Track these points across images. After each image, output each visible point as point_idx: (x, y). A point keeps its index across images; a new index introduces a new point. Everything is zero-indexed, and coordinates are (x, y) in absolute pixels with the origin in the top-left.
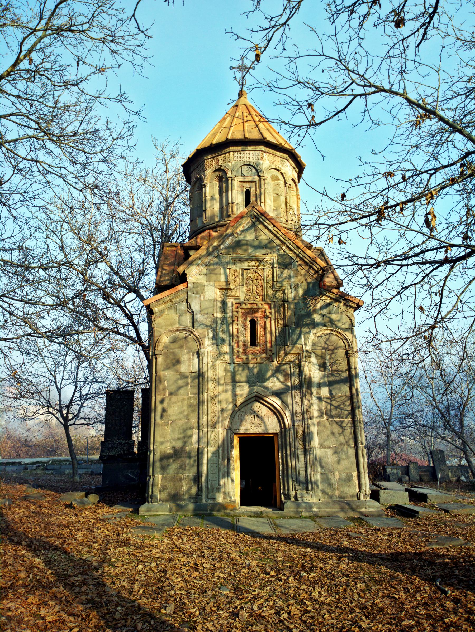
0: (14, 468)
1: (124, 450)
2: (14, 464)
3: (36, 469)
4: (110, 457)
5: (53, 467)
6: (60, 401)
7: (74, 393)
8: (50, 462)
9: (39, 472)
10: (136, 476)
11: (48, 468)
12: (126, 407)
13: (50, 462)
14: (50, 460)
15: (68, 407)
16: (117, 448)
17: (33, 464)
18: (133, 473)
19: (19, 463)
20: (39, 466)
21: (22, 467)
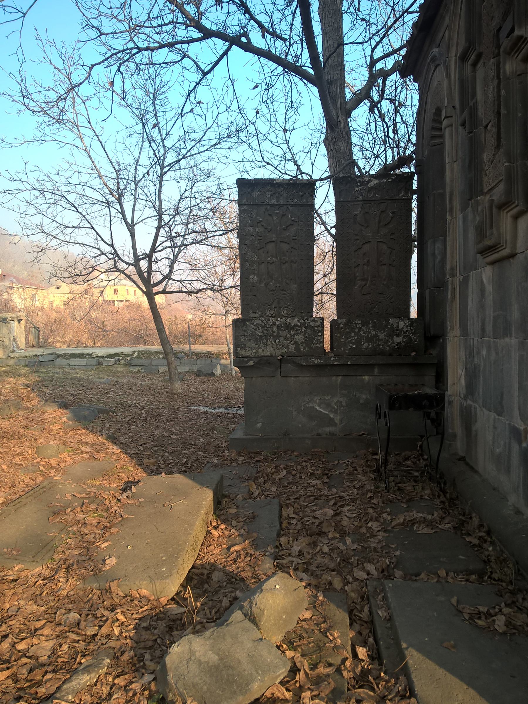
0: (82, 362)
1: (296, 343)
2: (81, 356)
4: (263, 362)
5: (139, 361)
6: (134, 247)
7: (158, 229)
8: (136, 355)
9: (120, 369)
10: (335, 412)
11: (133, 362)
12: (293, 229)
13: (136, 355)
14: (134, 352)
15: (149, 256)
16: (278, 337)
17: (110, 356)
18: (328, 405)
19: (90, 355)
20: (119, 360)
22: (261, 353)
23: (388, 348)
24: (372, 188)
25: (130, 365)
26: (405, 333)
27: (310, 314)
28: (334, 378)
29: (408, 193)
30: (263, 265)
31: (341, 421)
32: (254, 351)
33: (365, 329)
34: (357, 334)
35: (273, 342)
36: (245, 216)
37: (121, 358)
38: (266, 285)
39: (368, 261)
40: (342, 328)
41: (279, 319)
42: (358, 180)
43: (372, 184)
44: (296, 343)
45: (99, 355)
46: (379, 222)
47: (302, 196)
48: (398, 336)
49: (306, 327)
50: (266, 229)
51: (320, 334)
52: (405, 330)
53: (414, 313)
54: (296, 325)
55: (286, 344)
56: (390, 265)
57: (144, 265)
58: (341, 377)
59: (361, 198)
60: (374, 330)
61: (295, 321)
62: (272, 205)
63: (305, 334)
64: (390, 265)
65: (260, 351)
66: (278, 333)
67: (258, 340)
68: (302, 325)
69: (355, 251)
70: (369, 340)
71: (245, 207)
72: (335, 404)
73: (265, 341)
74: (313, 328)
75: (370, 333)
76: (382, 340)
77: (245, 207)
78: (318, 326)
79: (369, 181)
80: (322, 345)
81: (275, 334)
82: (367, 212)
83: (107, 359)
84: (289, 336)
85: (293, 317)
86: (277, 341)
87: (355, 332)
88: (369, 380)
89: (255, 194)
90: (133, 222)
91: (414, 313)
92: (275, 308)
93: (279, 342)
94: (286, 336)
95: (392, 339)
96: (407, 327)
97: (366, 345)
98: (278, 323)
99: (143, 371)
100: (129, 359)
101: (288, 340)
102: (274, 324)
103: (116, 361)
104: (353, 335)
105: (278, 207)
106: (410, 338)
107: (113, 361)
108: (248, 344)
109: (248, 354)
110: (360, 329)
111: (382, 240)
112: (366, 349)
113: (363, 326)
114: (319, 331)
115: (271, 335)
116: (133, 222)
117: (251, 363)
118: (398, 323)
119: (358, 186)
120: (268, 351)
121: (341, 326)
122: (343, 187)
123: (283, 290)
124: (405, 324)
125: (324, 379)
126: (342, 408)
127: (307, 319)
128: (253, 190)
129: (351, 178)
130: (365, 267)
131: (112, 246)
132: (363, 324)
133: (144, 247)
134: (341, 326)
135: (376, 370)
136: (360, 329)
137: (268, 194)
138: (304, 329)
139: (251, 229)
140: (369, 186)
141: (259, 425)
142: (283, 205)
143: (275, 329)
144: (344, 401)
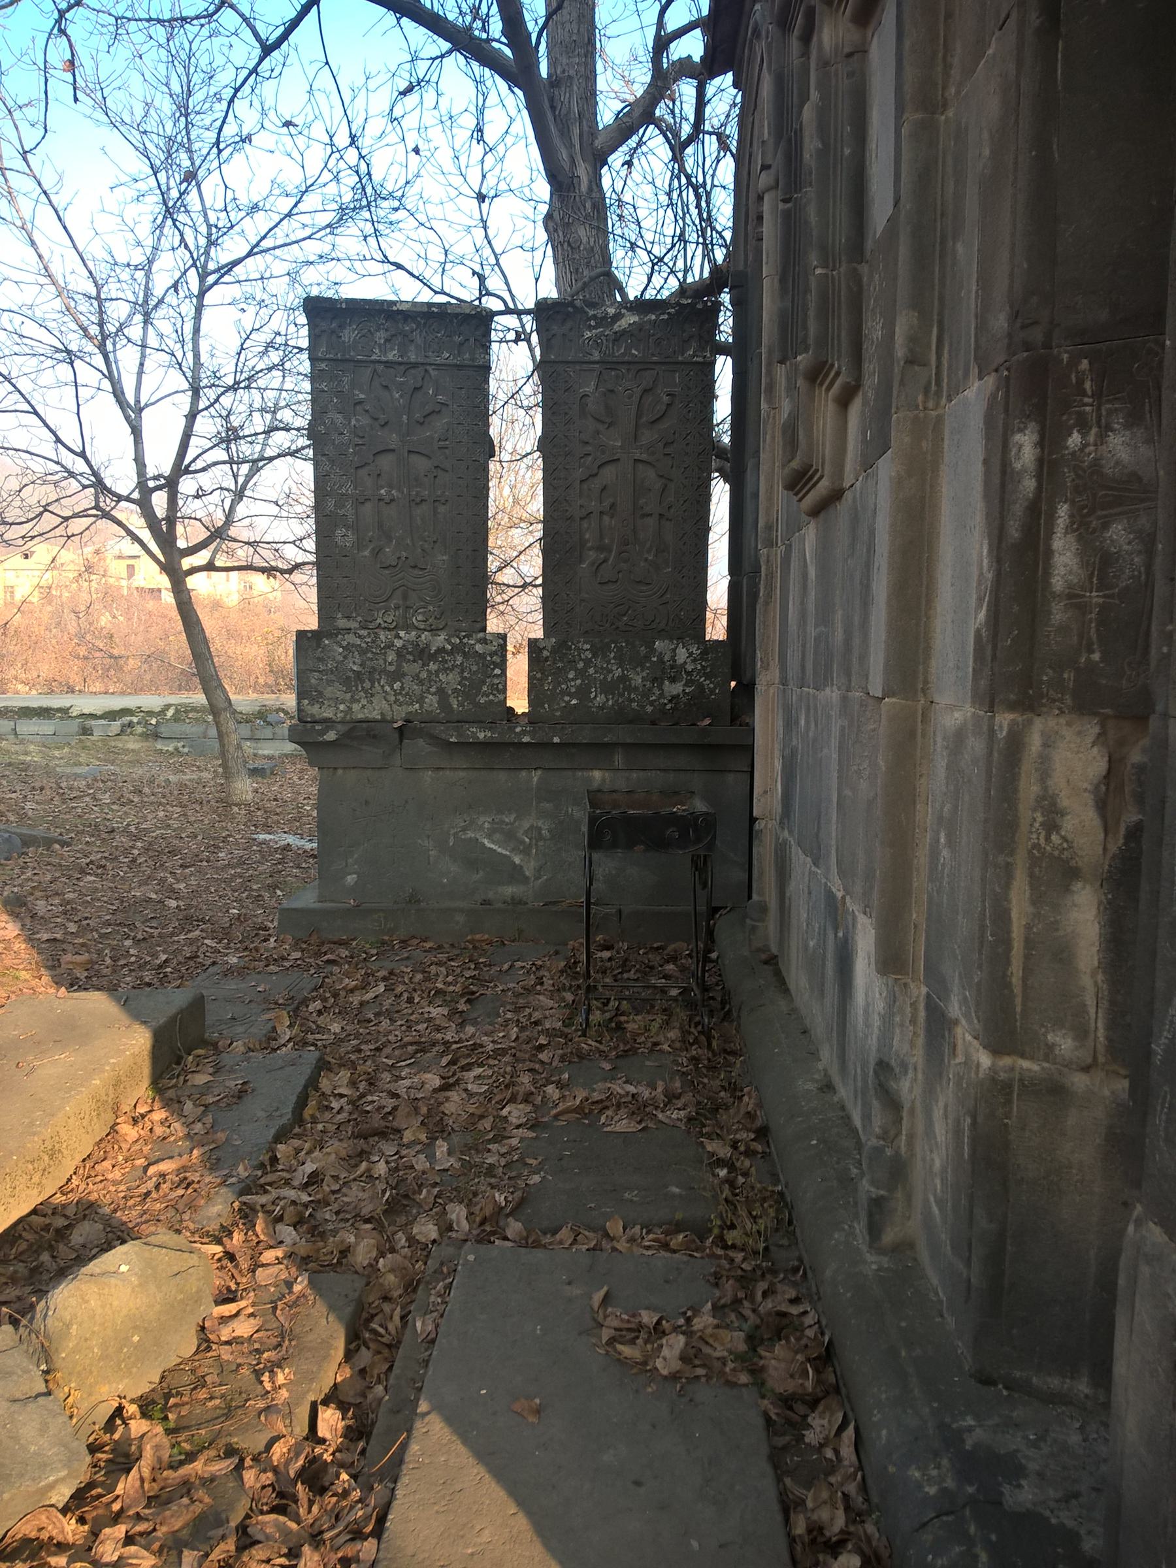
0: (46, 727)
1: (441, 692)
2: (44, 713)
3: (122, 732)
4: (360, 734)
5: (178, 729)
6: (140, 461)
7: (191, 417)
8: (170, 713)
9: (132, 744)
10: (526, 851)
11: (164, 731)
12: (440, 423)
13: (170, 713)
16: (398, 675)
17: (111, 715)
18: (509, 836)
19: (65, 711)
20: (130, 725)
21: (74, 726)
22: (359, 711)
23: (649, 709)
24: (623, 333)
25: (157, 736)
26: (689, 673)
27: (478, 626)
28: (524, 773)
29: (704, 349)
30: (368, 505)
31: (539, 871)
32: (342, 707)
33: (598, 662)
34: (581, 674)
35: (387, 688)
36: (324, 386)
37: (135, 720)
38: (377, 552)
39: (613, 506)
40: (546, 659)
41: (402, 634)
42: (591, 313)
44: (441, 692)
45: (86, 711)
46: (639, 416)
47: (461, 344)
48: (673, 680)
49: (465, 655)
50: (376, 419)
51: (497, 671)
52: (689, 668)
53: (717, 629)
54: (441, 650)
55: (418, 692)
57: (159, 501)
58: (539, 772)
59: (596, 356)
60: (620, 665)
61: (440, 640)
62: (389, 364)
63: (462, 671)
65: (356, 707)
66: (399, 666)
67: (352, 682)
68: (456, 649)
70: (608, 688)
71: (323, 366)
72: (526, 833)
73: (367, 685)
74: (482, 656)
75: (610, 671)
76: (636, 688)
77: (323, 366)
78: (492, 654)
79: (617, 317)
80: (501, 697)
81: (392, 668)
82: (612, 391)
83: (103, 722)
84: (424, 675)
85: (434, 631)
86: (397, 685)
87: (576, 670)
88: (604, 780)
89: (349, 335)
90: (138, 401)
91: (717, 629)
92: (397, 608)
93: (402, 688)
94: (417, 675)
97: (601, 699)
98: (398, 643)
99: (186, 750)
100: (154, 721)
101: (421, 682)
102: (390, 646)
103: (123, 726)
104: (571, 676)
105: (402, 368)
106: (701, 687)
107: (116, 726)
108: (329, 691)
109: (328, 714)
110: (588, 662)
111: (644, 457)
112: (602, 708)
114: (496, 665)
115: (384, 671)
116: (138, 401)
117: (331, 736)
118: (674, 650)
119: (590, 328)
120: (374, 707)
121: (546, 653)
122: (555, 328)
123: (415, 567)
124: (691, 654)
125: (502, 776)
126: (541, 843)
127: (468, 636)
128: (342, 327)
129: (574, 307)
130: (606, 518)
131: (82, 455)
132: (595, 652)
133: (160, 461)
134: (546, 653)
135: (619, 759)
136: (588, 662)
137: (380, 336)
138: (459, 659)
139: (339, 419)
140: (616, 327)
141: (351, 879)
142: (415, 365)
143: (391, 656)
144: (545, 826)
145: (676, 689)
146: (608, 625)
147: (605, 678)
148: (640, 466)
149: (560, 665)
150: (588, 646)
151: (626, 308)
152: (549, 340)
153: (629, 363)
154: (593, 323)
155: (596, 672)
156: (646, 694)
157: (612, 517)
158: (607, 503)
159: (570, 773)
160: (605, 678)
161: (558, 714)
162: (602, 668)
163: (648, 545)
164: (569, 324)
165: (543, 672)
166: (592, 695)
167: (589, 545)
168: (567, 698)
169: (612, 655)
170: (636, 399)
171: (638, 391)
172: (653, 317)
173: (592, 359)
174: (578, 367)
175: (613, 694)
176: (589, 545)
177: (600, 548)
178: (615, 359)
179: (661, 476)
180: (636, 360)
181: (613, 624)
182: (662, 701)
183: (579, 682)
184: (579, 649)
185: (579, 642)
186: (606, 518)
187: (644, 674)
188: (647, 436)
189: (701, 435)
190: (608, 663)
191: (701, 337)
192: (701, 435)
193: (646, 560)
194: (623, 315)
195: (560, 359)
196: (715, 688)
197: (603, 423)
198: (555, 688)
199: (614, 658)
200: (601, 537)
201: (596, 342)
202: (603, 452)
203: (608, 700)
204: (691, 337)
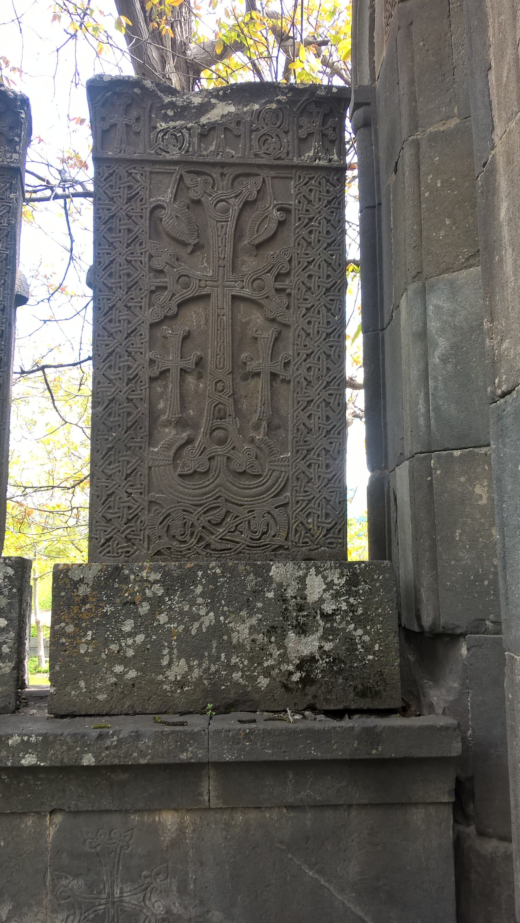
23: (263, 682)
24: (212, 127)
28: (29, 821)
29: (327, 151)
33: (176, 602)
34: (144, 624)
39: (199, 362)
40: (84, 600)
42: (167, 100)
43: (214, 115)
48: (302, 630)
52: (329, 608)
53: (358, 547)
56: (274, 376)
58: (58, 818)
59: (175, 154)
60: (212, 607)
64: (274, 376)
69: (153, 326)
70: (192, 648)
75: (196, 618)
76: (239, 647)
79: (204, 108)
82: (198, 202)
87: (136, 616)
88: (181, 829)
91: (358, 547)
95: (281, 646)
96: (336, 596)
97: (180, 667)
104: (128, 626)
106: (350, 641)
110: (157, 604)
111: (247, 292)
112: (180, 684)
113: (169, 591)
118: (302, 580)
119: (166, 118)
121: (83, 590)
124: (330, 585)
129: (143, 88)
132: (170, 583)
134: (83, 590)
135: (209, 789)
136: (157, 604)
140: (204, 120)
145: (309, 645)
146: (194, 540)
147: (187, 630)
148: (242, 307)
149: (108, 609)
150: (153, 577)
151: (217, 97)
152: (105, 132)
153: (223, 165)
154: (170, 113)
155: (171, 620)
156: (257, 655)
157: (200, 377)
158: (193, 359)
159: (116, 819)
160: (187, 630)
161: (102, 697)
162: (181, 613)
163: (255, 418)
164: (134, 113)
165: (77, 621)
166: (165, 662)
167: (164, 418)
168: (119, 669)
169: (199, 590)
170: (233, 212)
171: (236, 205)
172: (257, 107)
173: (168, 157)
174: (148, 169)
175: (201, 658)
176: (164, 418)
177: (181, 423)
178: (201, 159)
179: (273, 320)
180: (232, 160)
181: (201, 539)
182: (285, 667)
183: (140, 638)
184: (142, 580)
185: (142, 568)
186: (191, 380)
187: (254, 621)
188: (250, 264)
189: (329, 264)
190: (193, 603)
191: (324, 135)
192: (329, 264)
193: (252, 441)
194: (214, 106)
195: (122, 155)
196: (373, 641)
197: (184, 244)
198: (98, 651)
199: (203, 595)
200: (183, 407)
201: (175, 135)
202: (186, 286)
203: (191, 668)
204: (310, 135)
